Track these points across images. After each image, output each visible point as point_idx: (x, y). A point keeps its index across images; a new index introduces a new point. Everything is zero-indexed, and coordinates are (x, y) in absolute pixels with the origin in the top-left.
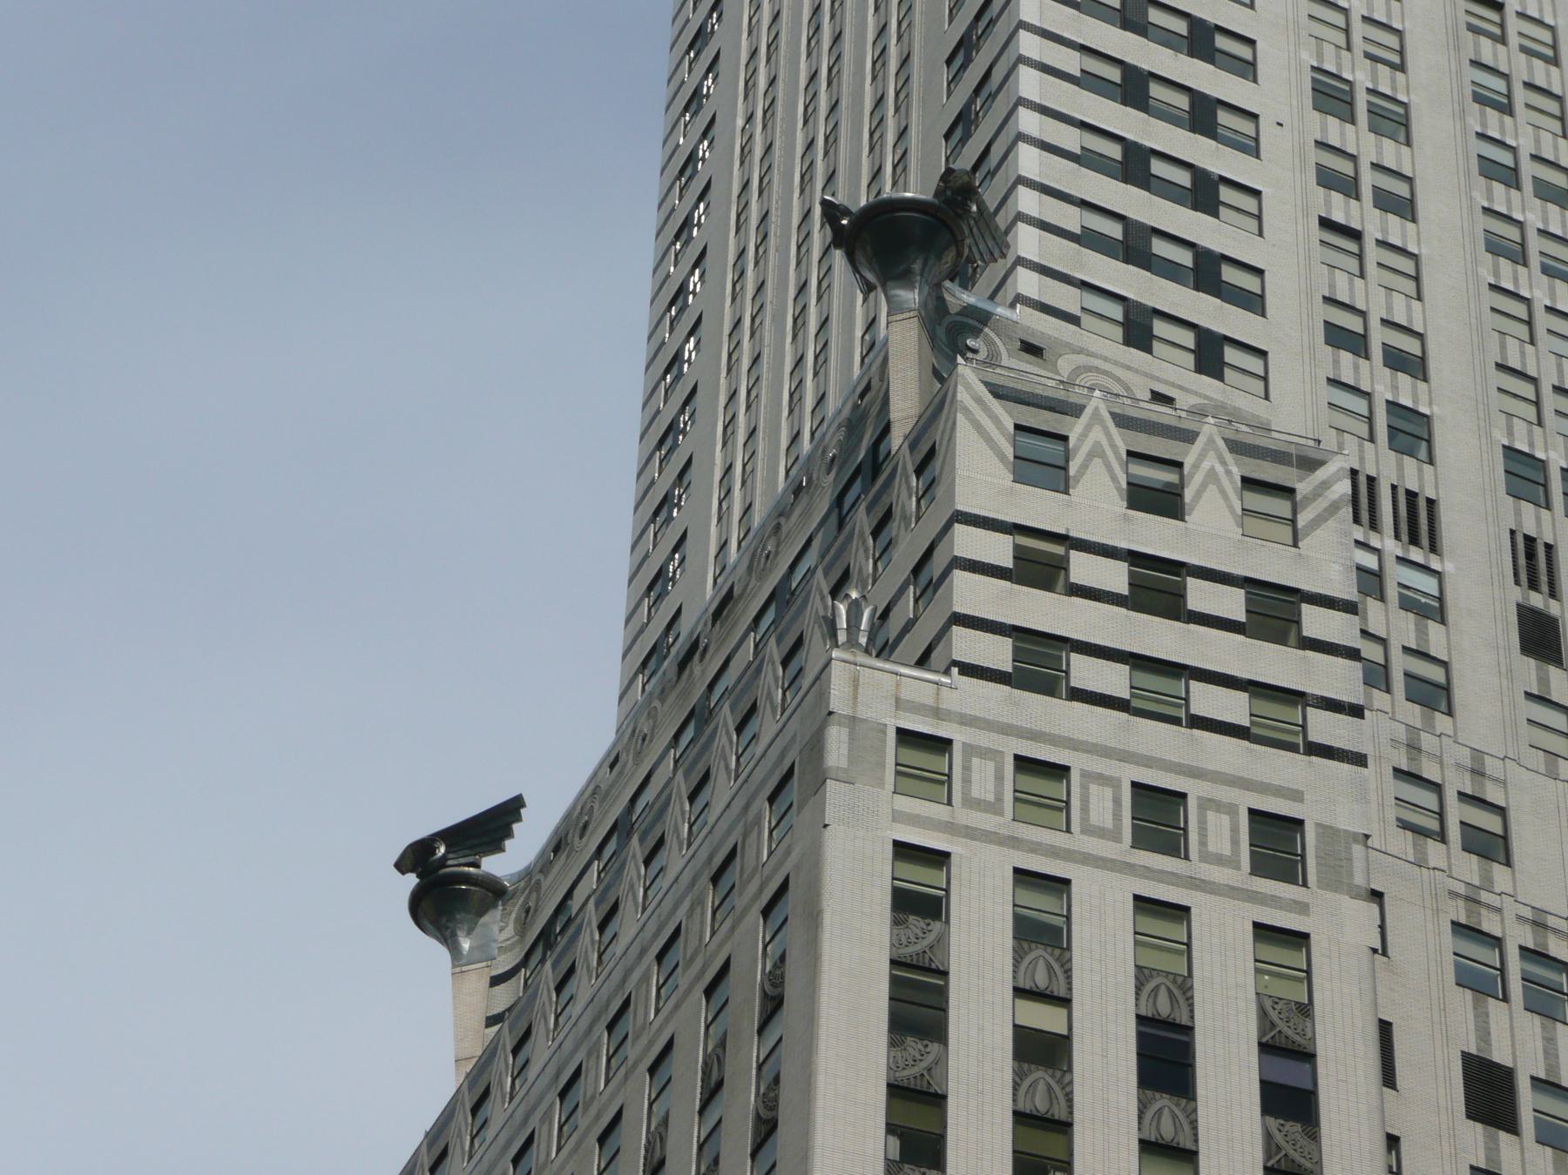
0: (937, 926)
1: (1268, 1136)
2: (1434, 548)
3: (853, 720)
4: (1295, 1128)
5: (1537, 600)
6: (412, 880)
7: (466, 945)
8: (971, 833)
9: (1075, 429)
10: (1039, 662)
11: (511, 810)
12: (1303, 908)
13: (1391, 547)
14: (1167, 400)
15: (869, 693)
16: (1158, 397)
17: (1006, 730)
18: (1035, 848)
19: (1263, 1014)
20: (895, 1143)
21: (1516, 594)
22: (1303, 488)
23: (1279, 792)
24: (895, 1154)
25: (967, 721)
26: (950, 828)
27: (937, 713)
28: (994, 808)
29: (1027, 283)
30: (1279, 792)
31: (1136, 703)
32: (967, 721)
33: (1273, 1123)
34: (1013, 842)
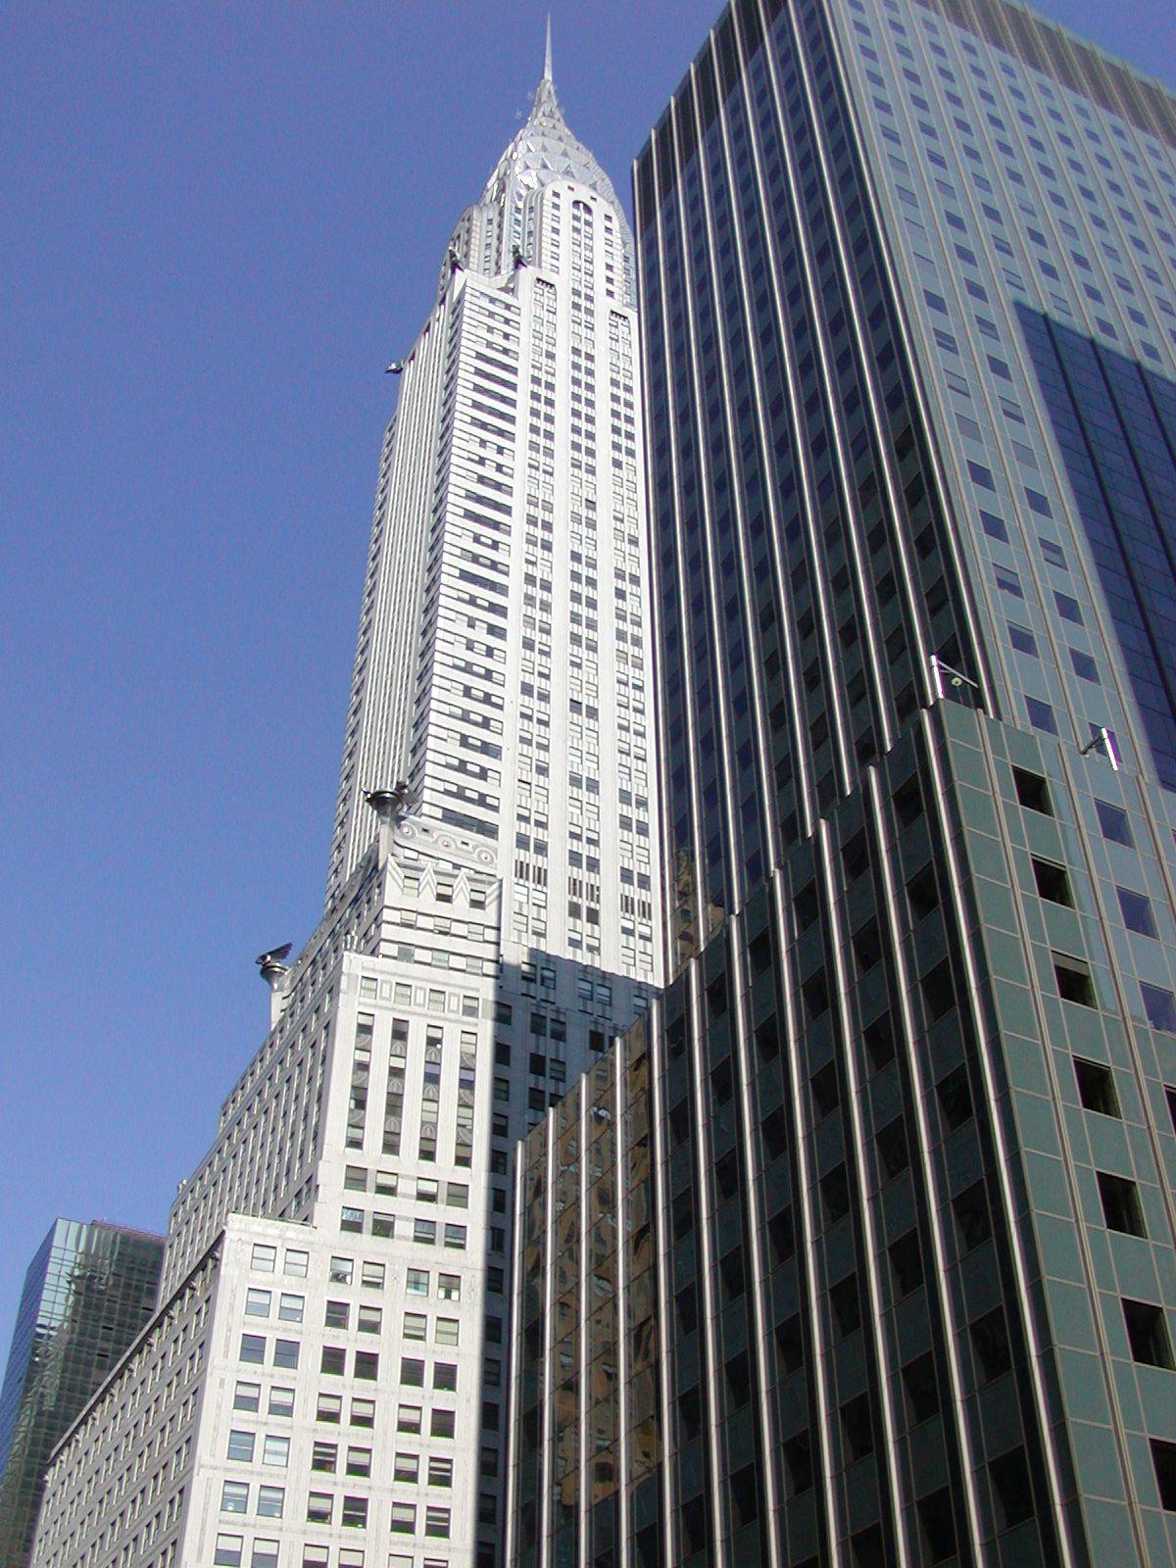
0: (369, 1036)
1: (459, 1094)
2: (545, 885)
3: (349, 975)
4: (468, 1092)
5: (575, 899)
6: (261, 966)
7: (276, 986)
8: (381, 1007)
9: (421, 876)
10: (406, 952)
11: (288, 946)
12: (476, 1025)
13: (532, 886)
14: (467, 844)
15: (354, 963)
16: (463, 843)
17: (394, 974)
18: (400, 1011)
19: (462, 1058)
20: (353, 1102)
21: (569, 897)
22: (488, 891)
23: (473, 989)
24: (353, 1107)
25: (382, 972)
26: (375, 1006)
27: (374, 970)
28: (389, 999)
29: (426, 809)
30: (473, 989)
31: (434, 963)
32: (382, 972)
33: (462, 1091)
34: (394, 1009)
